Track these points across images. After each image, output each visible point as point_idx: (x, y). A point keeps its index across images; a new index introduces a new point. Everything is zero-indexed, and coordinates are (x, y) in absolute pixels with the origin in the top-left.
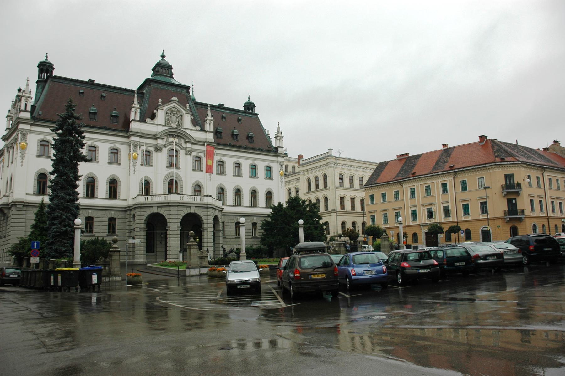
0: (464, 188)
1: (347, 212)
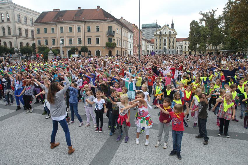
0: (89, 31)
1: (23, 37)
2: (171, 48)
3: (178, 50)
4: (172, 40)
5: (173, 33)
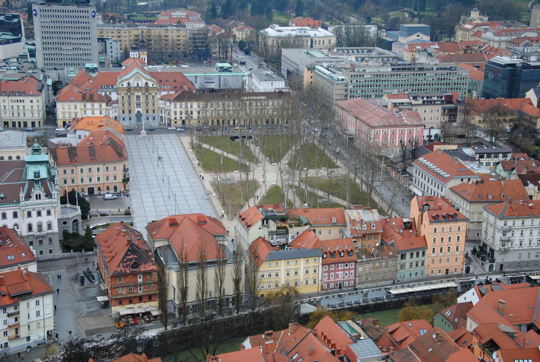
2: (150, 111)
3: (163, 115)
4: (150, 98)
5: (153, 85)
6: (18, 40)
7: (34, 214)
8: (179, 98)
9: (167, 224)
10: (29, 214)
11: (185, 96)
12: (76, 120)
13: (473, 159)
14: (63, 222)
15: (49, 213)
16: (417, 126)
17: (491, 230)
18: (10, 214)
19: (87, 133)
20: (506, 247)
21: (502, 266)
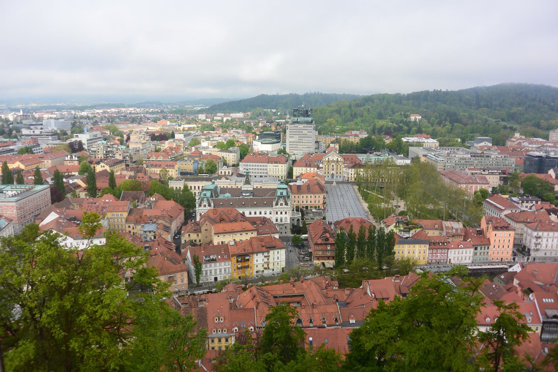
6: (279, 142)
7: (279, 213)
8: (353, 167)
9: (344, 222)
10: (277, 213)
11: (356, 165)
12: (302, 174)
13: (518, 203)
14: (292, 219)
15: (286, 213)
16: (485, 184)
17: (529, 238)
18: (268, 212)
19: (307, 180)
20: (537, 248)
21: (534, 259)
